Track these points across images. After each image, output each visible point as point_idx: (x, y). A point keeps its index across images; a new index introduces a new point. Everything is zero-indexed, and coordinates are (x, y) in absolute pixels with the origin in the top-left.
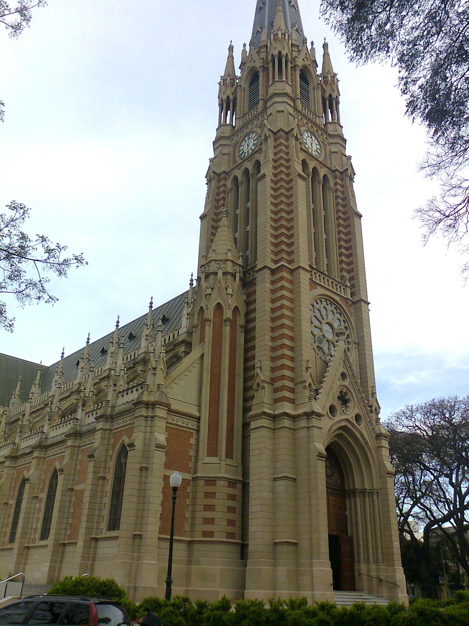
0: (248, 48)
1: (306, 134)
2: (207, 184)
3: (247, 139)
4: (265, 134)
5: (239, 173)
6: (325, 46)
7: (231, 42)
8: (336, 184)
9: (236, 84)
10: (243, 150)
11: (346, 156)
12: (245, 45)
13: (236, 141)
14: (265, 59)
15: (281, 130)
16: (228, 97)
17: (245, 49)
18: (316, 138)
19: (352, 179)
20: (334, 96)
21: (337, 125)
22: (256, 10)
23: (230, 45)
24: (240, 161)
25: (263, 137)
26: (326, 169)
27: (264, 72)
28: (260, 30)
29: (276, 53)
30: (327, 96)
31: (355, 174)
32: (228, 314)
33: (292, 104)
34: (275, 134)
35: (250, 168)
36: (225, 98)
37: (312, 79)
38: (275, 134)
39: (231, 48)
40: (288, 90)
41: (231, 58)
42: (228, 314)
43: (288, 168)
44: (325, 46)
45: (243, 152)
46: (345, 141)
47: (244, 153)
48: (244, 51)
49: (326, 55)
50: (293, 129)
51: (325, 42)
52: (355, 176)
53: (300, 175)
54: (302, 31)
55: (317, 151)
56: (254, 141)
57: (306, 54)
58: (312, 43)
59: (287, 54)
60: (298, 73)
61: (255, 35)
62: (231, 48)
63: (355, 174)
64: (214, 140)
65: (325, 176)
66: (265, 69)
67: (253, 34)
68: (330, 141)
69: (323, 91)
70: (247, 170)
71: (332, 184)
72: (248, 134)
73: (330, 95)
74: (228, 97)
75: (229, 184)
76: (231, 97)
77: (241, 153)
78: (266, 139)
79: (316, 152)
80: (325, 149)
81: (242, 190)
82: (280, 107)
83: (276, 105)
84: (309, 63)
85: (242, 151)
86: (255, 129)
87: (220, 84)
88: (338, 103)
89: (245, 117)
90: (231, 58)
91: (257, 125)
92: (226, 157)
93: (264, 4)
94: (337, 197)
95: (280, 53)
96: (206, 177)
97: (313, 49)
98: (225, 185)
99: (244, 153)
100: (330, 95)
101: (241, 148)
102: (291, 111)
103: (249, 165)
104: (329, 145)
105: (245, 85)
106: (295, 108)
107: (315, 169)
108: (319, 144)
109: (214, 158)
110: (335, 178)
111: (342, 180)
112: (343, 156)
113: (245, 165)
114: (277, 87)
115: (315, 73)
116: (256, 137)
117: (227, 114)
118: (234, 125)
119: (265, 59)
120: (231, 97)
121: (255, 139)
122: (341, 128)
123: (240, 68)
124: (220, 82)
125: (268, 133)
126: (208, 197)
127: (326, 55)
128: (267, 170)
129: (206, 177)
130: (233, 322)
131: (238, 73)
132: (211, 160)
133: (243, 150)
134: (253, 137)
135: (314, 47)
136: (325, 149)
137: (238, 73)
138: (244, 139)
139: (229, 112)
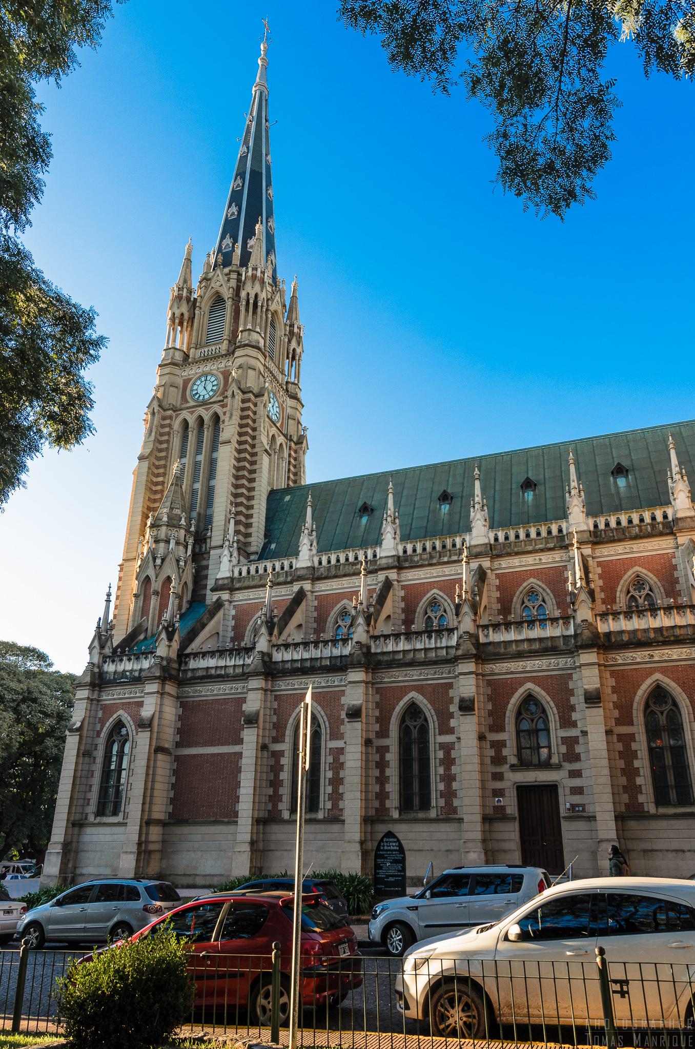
3: (203, 379)
16: (182, 315)
24: (192, 403)
33: (263, 361)
35: (206, 418)
36: (177, 314)
43: (254, 438)
53: (266, 451)
74: (182, 315)
77: (194, 392)
86: (215, 372)
95: (256, 296)
98: (170, 426)
101: (195, 387)
128: (229, 430)
138: (199, 378)
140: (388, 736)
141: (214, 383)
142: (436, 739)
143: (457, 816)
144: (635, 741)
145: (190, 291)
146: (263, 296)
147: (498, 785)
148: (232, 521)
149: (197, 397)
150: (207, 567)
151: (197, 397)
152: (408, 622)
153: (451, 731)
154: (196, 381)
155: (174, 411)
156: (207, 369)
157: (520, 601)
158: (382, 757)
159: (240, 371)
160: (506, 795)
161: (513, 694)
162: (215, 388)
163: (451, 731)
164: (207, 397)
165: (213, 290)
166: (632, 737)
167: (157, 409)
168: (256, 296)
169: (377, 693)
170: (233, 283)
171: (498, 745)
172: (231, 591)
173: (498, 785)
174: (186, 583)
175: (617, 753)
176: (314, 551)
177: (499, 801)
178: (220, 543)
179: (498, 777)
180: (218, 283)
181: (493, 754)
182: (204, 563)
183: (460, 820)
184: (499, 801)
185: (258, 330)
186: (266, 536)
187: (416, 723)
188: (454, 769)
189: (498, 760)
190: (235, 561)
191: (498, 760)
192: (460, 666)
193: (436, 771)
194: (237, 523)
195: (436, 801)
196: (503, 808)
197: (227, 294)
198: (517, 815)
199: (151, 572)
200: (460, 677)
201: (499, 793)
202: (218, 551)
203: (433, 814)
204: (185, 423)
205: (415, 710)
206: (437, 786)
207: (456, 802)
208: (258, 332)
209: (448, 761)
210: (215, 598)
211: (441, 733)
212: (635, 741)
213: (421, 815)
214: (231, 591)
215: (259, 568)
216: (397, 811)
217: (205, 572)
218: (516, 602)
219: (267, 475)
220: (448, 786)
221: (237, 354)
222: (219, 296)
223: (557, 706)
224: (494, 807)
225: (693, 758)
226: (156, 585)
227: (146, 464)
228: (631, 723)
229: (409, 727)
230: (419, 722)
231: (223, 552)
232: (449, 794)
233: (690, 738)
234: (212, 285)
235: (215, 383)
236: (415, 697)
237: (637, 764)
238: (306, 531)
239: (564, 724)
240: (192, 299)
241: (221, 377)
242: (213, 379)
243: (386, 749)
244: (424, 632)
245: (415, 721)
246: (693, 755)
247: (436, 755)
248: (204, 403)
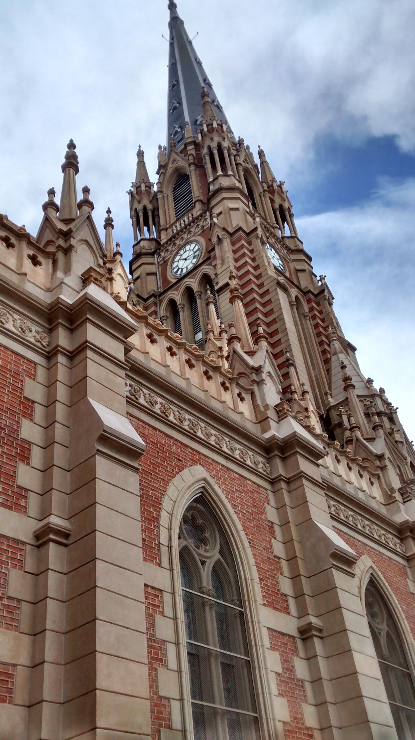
3: (182, 252)
4: (218, 236)
5: (177, 295)
7: (140, 146)
8: (311, 309)
10: (177, 266)
15: (240, 229)
16: (145, 208)
18: (276, 252)
19: (331, 304)
20: (286, 205)
21: (296, 239)
22: (170, 110)
25: (215, 240)
27: (196, 170)
30: (277, 206)
31: (333, 299)
34: (231, 235)
36: (140, 207)
37: (257, 186)
38: (231, 235)
39: (140, 154)
40: (238, 184)
41: (141, 164)
45: (179, 269)
46: (310, 259)
47: (180, 270)
50: (255, 229)
52: (333, 301)
57: (245, 155)
59: (228, 146)
60: (242, 173)
61: (172, 136)
62: (140, 154)
63: (333, 299)
65: (296, 297)
66: (199, 165)
67: (170, 135)
68: (293, 257)
69: (272, 201)
70: (189, 290)
71: (307, 310)
73: (281, 206)
74: (145, 208)
75: (162, 310)
76: (150, 207)
77: (175, 270)
78: (220, 240)
80: (288, 266)
81: (184, 316)
82: (232, 205)
83: (225, 201)
84: (251, 166)
85: (177, 268)
87: (131, 193)
89: (174, 228)
90: (141, 164)
92: (153, 277)
94: (316, 326)
99: (180, 270)
100: (281, 206)
101: (175, 265)
104: (291, 262)
105: (169, 192)
108: (281, 259)
110: (309, 301)
111: (318, 304)
114: (224, 182)
116: (197, 248)
120: (150, 207)
121: (195, 250)
122: (302, 244)
123: (157, 173)
124: (131, 190)
125: (221, 234)
133: (177, 266)
134: (192, 248)
136: (288, 266)
138: (177, 253)
145: (149, 186)
149: (179, 273)
151: (179, 273)
204: (172, 303)
242: (193, 246)
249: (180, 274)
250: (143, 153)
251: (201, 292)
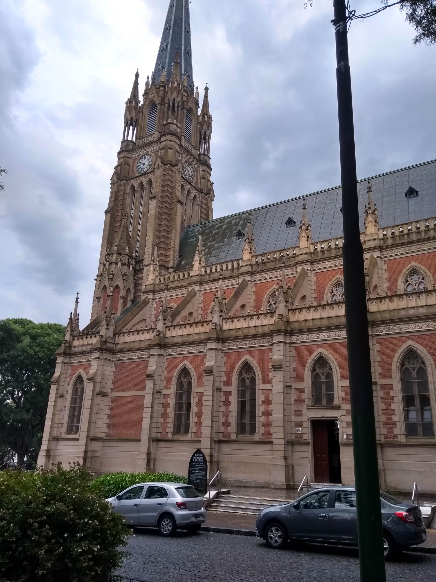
0: (150, 81)
1: (186, 164)
2: (110, 188)
6: (207, 89)
9: (138, 107)
11: (210, 182)
12: (148, 77)
13: (135, 157)
14: (162, 98)
17: (148, 80)
19: (212, 200)
20: (208, 133)
23: (137, 72)
26: (196, 191)
28: (161, 69)
29: (172, 98)
32: (122, 293)
33: (178, 142)
35: (145, 183)
39: (137, 75)
41: (136, 84)
42: (122, 293)
43: (171, 193)
44: (207, 89)
45: (140, 168)
46: (211, 169)
47: (141, 169)
48: (147, 83)
49: (206, 97)
51: (207, 86)
54: (192, 76)
55: (191, 177)
56: (149, 162)
58: (197, 88)
59: (179, 101)
62: (137, 75)
64: (119, 151)
70: (141, 184)
72: (144, 155)
77: (139, 167)
79: (191, 178)
85: (139, 167)
86: (150, 153)
88: (209, 138)
90: (136, 84)
91: (152, 150)
93: (167, 46)
95: (174, 100)
96: (111, 180)
97: (197, 94)
99: (141, 169)
100: (205, 132)
101: (139, 164)
102: (178, 148)
103: (144, 180)
106: (181, 145)
107: (189, 191)
109: (118, 166)
112: (208, 182)
113: (141, 180)
115: (197, 114)
117: (129, 129)
118: (134, 141)
119: (162, 98)
126: (111, 197)
127: (206, 97)
129: (111, 180)
130: (125, 298)
131: (141, 99)
132: (116, 168)
135: (199, 91)
137: (141, 99)
138: (141, 158)
139: (131, 127)
140: (231, 385)
141: (150, 160)
142: (260, 387)
143: (270, 440)
144: (393, 390)
145: (137, 102)
146: (178, 99)
147: (298, 419)
148: (156, 248)
149: (140, 170)
150: (141, 278)
151: (140, 170)
152: (257, 308)
153: (269, 381)
154: (139, 160)
155: (127, 181)
156: (145, 152)
157: (330, 291)
158: (227, 399)
159: (163, 151)
160: (304, 426)
161: (310, 356)
162: (150, 163)
163: (269, 381)
164: (145, 169)
165: (150, 100)
166: (390, 386)
167: (116, 180)
168: (174, 100)
169: (225, 356)
170: (161, 93)
171: (300, 391)
172: (154, 293)
173: (298, 419)
174: (129, 289)
175: (379, 398)
176: (203, 264)
177: (299, 430)
178: (149, 262)
179: (298, 413)
180: (153, 94)
181: (296, 397)
182: (141, 275)
183: (272, 443)
184: (299, 430)
185: (175, 122)
186: (180, 256)
187: (249, 376)
188: (271, 408)
189: (299, 401)
190: (157, 274)
191: (299, 401)
192: (274, 337)
193: (260, 408)
194: (159, 249)
195: (259, 429)
196: (301, 435)
197: (157, 101)
198: (310, 441)
199: (107, 283)
200: (274, 345)
201: (299, 424)
202: (148, 268)
203: (256, 437)
205: (249, 367)
206: (260, 419)
207: (271, 430)
208: (175, 124)
209: (267, 402)
210: (144, 297)
211: (263, 383)
212: (393, 390)
213: (249, 438)
214: (154, 293)
215: (170, 277)
216: (235, 435)
217: (140, 282)
218: (327, 292)
219: (180, 217)
220: (267, 419)
221: (162, 140)
222: (154, 103)
223: (339, 364)
224: (295, 434)
225: (435, 403)
226: (109, 291)
227: (109, 215)
228: (390, 376)
229: (244, 378)
230: (251, 375)
231: (150, 268)
232: (267, 425)
233: (433, 388)
234: (150, 97)
235: (150, 160)
236: (248, 359)
237: (393, 406)
238: (197, 252)
239: (344, 377)
240: (138, 107)
241: (153, 155)
242: (149, 157)
243: (229, 393)
244: (267, 313)
245: (249, 375)
246: (434, 401)
247: (260, 397)
248: (144, 174)
249: (140, 171)
250: (139, 75)
251: (147, 188)
